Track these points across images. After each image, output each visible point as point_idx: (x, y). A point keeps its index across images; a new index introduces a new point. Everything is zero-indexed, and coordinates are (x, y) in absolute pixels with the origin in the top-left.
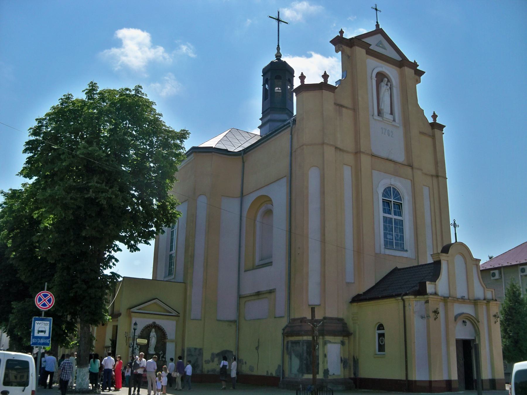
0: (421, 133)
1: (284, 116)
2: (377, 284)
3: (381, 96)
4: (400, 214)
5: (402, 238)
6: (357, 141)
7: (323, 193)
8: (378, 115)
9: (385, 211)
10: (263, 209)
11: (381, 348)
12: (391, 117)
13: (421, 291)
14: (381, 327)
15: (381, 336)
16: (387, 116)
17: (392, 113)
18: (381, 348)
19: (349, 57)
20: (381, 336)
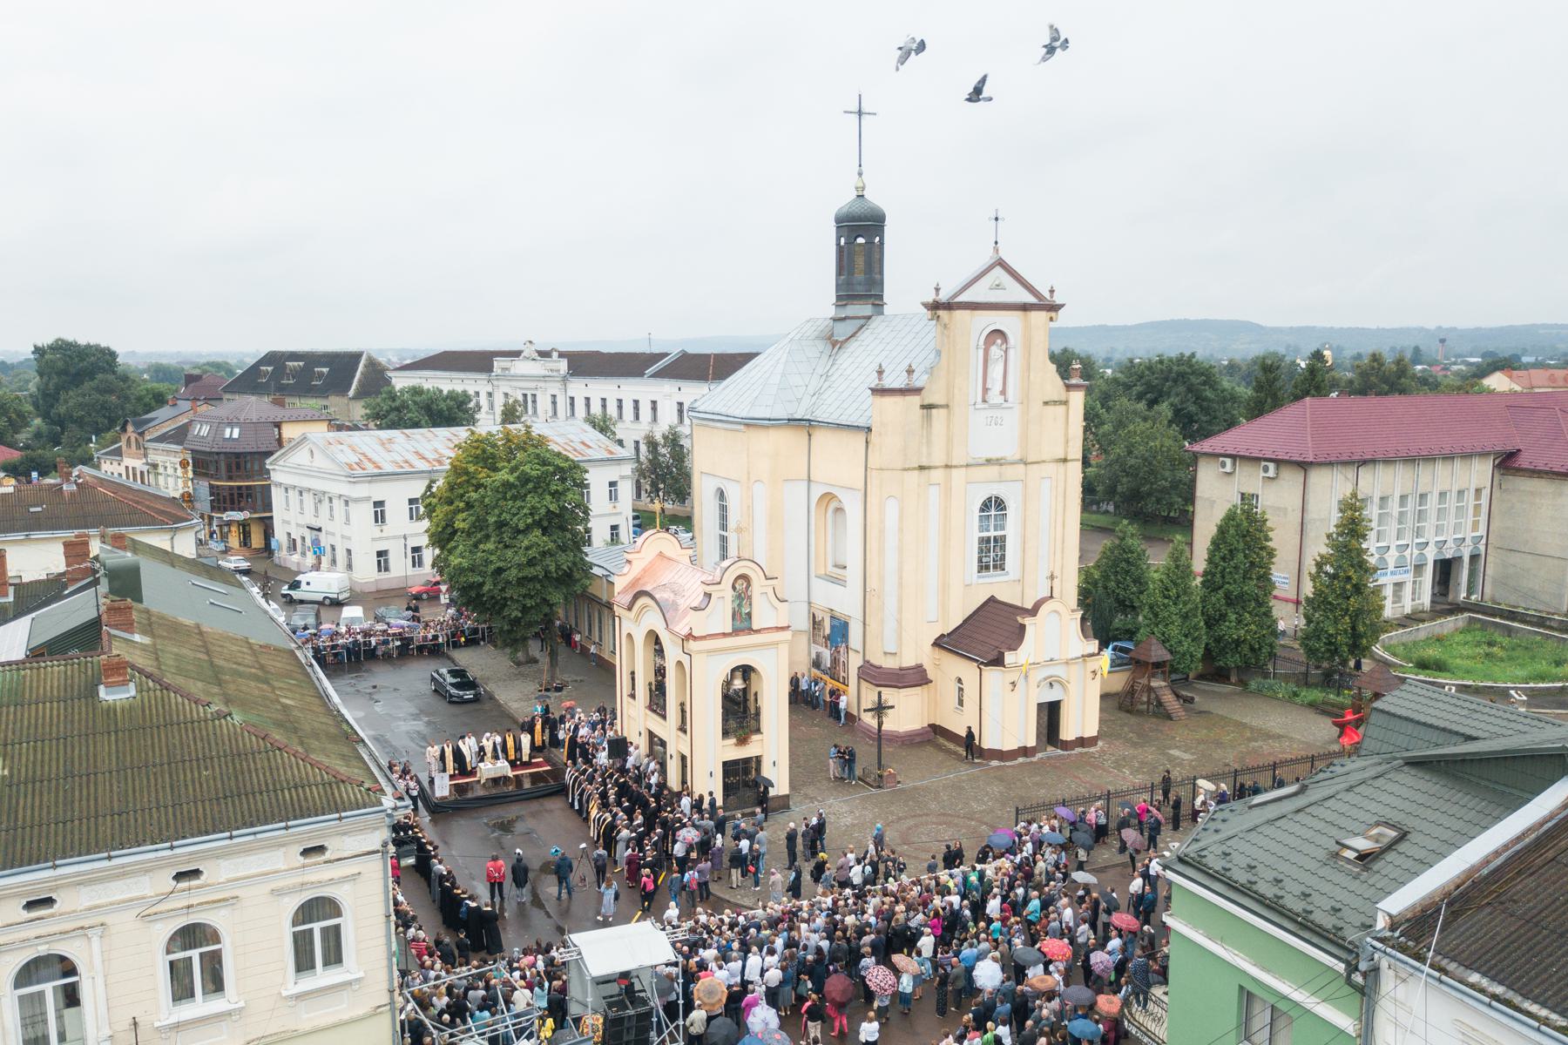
0: (1046, 403)
1: (866, 310)
2: (965, 621)
3: (990, 369)
4: (1003, 528)
5: (1003, 558)
6: (948, 454)
7: (901, 530)
8: (984, 401)
9: (981, 531)
10: (833, 505)
11: (961, 703)
12: (1000, 399)
13: (998, 661)
14: (960, 681)
15: (961, 690)
16: (995, 397)
17: (1003, 392)
18: (961, 703)
19: (945, 326)
20: (961, 690)
